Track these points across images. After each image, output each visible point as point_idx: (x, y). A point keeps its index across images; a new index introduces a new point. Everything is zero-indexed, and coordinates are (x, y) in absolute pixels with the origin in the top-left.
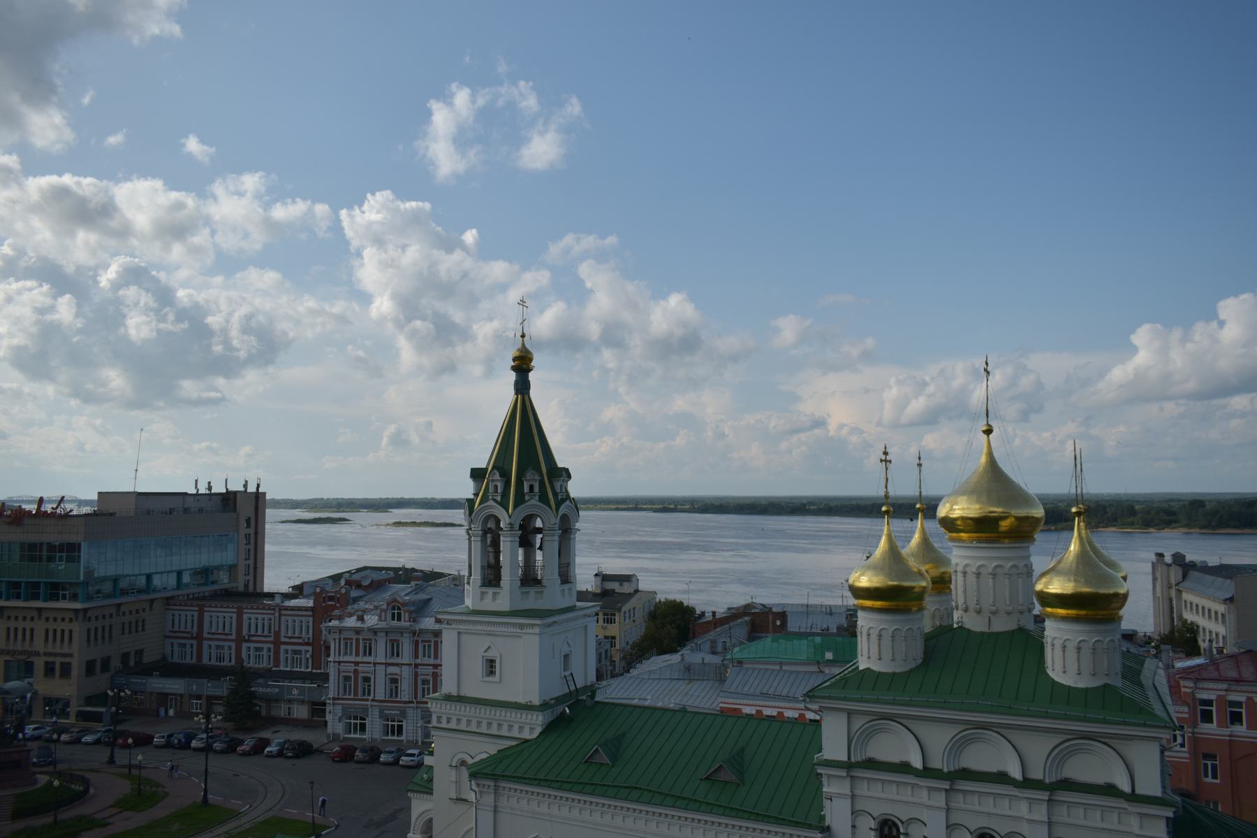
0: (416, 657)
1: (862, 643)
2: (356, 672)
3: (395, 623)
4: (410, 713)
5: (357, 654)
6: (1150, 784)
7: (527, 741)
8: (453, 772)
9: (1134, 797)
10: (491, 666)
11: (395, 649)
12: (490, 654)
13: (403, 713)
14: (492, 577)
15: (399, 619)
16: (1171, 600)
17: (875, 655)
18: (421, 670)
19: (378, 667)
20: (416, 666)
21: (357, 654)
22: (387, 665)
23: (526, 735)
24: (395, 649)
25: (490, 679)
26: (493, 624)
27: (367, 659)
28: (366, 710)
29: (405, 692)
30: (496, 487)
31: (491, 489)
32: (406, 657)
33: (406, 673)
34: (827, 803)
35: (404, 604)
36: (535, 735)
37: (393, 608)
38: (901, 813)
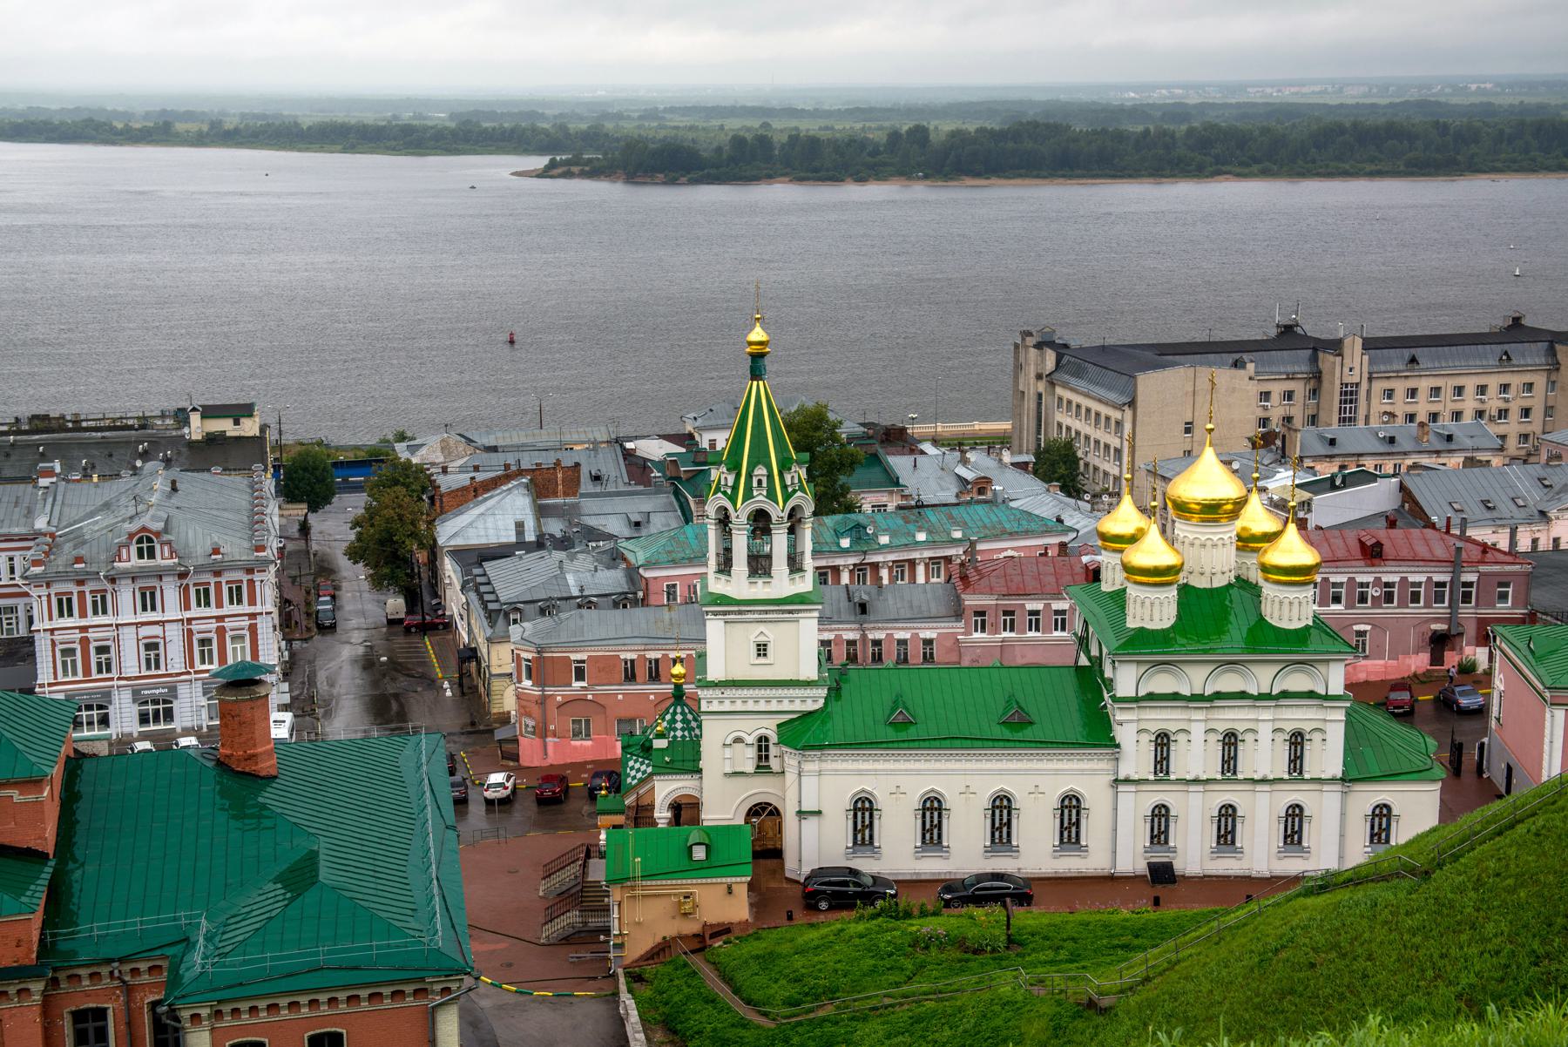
0: (187, 608)
1: (1131, 609)
2: (85, 642)
3: (145, 562)
4: (183, 690)
5: (83, 615)
6: (1337, 686)
7: (810, 713)
8: (728, 752)
9: (1327, 698)
10: (762, 649)
11: (148, 600)
12: (762, 639)
13: (173, 690)
14: (759, 565)
15: (152, 555)
16: (1040, 396)
17: (1147, 618)
18: (195, 627)
19: (126, 630)
20: (190, 620)
21: (83, 615)
22: (138, 625)
23: (810, 706)
24: (148, 600)
25: (762, 660)
26: (766, 612)
27: (101, 619)
28: (107, 694)
29: (174, 658)
30: (760, 482)
31: (755, 484)
32: (173, 611)
33: (174, 634)
34: (1116, 727)
35: (158, 534)
36: (821, 703)
37: (140, 541)
38: (1171, 727)
